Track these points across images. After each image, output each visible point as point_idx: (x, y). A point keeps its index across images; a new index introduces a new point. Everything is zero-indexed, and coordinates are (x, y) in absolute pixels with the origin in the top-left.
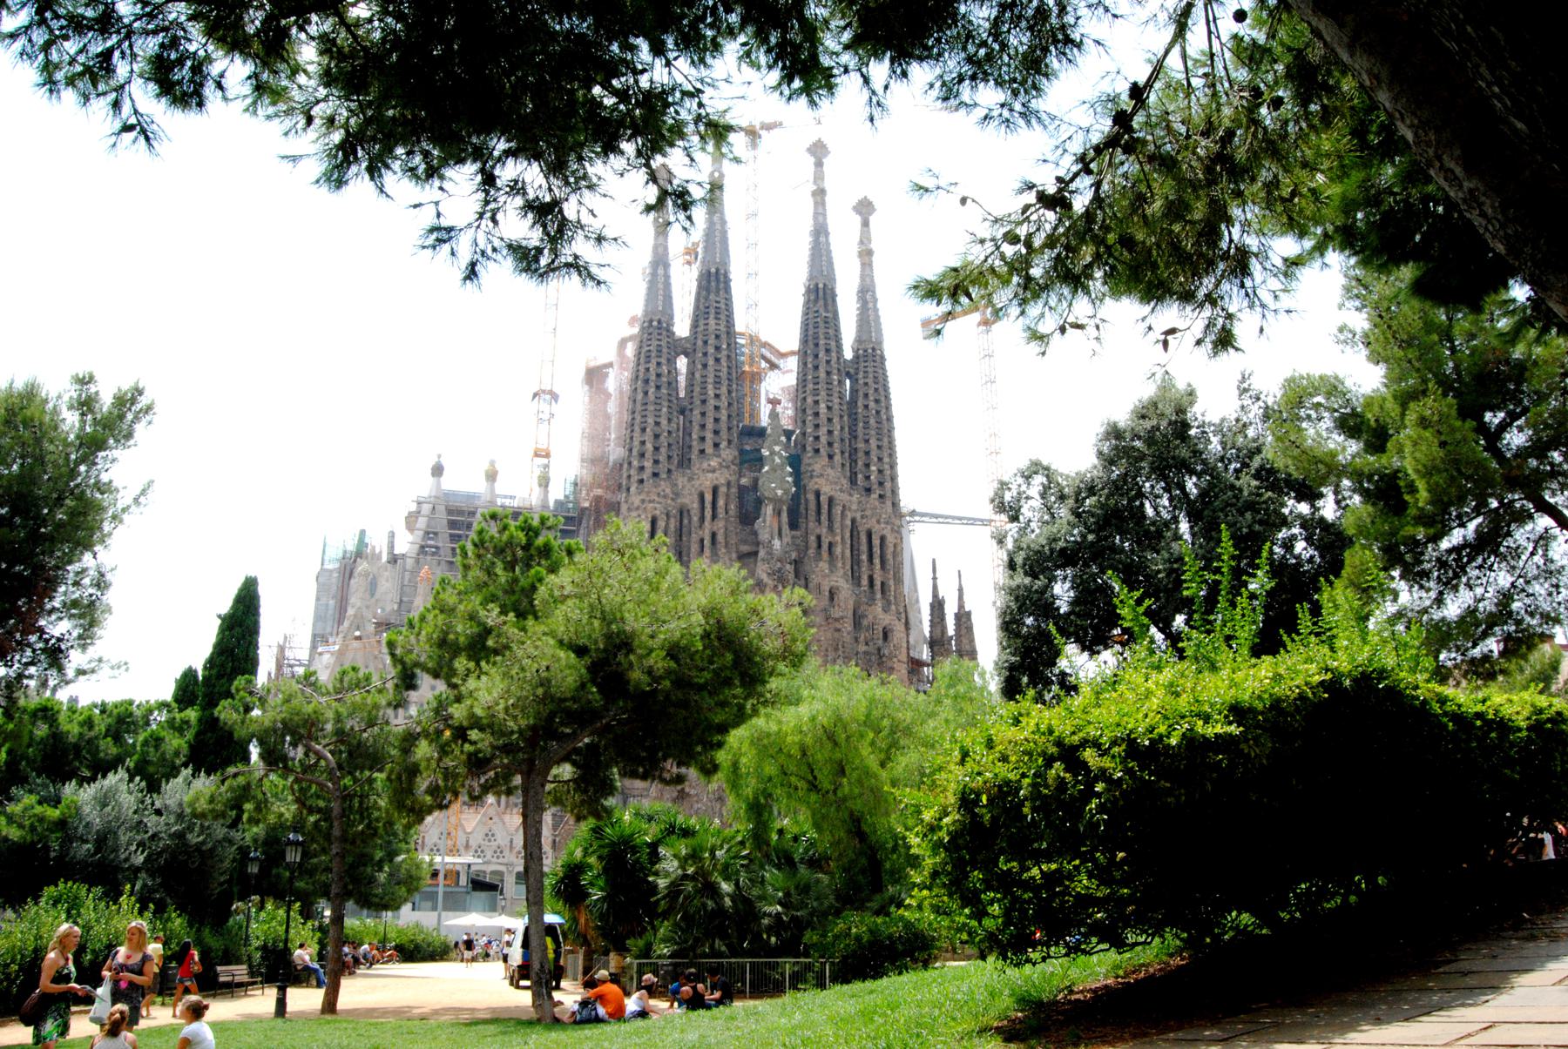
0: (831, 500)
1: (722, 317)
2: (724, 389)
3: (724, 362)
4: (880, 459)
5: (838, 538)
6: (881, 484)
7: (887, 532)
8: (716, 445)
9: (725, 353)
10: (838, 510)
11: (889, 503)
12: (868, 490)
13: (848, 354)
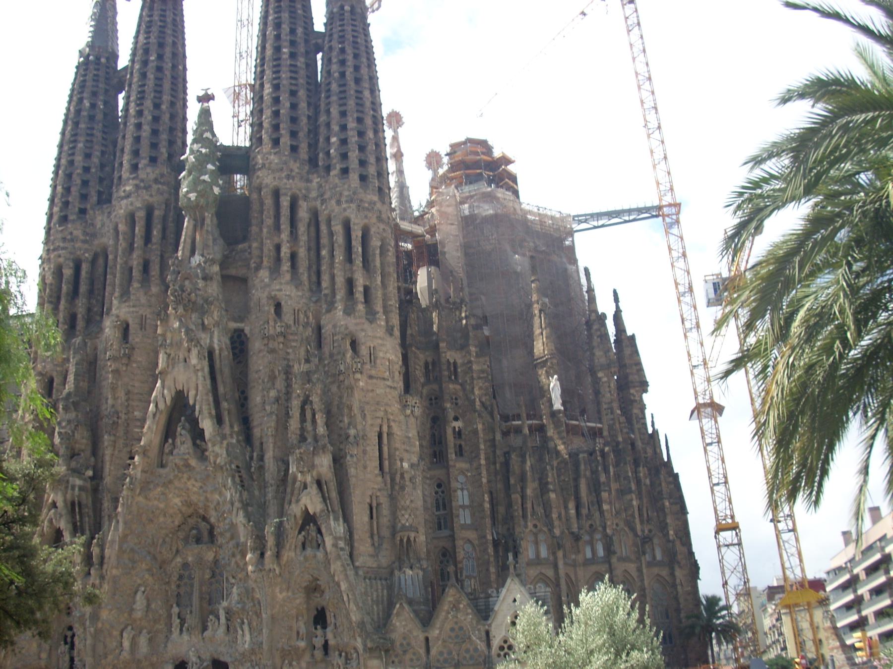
0: (276, 194)
1: (155, 29)
2: (148, 103)
3: (151, 76)
4: (344, 128)
5: (285, 236)
6: (344, 156)
7: (352, 213)
8: (135, 168)
9: (154, 64)
10: (285, 202)
11: (354, 177)
12: (328, 169)
13: (319, 24)
